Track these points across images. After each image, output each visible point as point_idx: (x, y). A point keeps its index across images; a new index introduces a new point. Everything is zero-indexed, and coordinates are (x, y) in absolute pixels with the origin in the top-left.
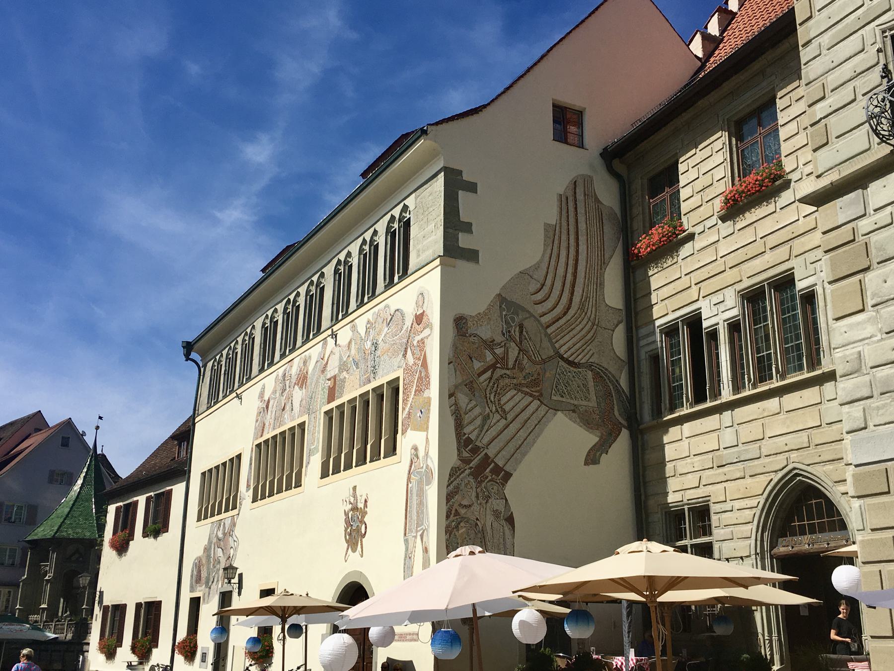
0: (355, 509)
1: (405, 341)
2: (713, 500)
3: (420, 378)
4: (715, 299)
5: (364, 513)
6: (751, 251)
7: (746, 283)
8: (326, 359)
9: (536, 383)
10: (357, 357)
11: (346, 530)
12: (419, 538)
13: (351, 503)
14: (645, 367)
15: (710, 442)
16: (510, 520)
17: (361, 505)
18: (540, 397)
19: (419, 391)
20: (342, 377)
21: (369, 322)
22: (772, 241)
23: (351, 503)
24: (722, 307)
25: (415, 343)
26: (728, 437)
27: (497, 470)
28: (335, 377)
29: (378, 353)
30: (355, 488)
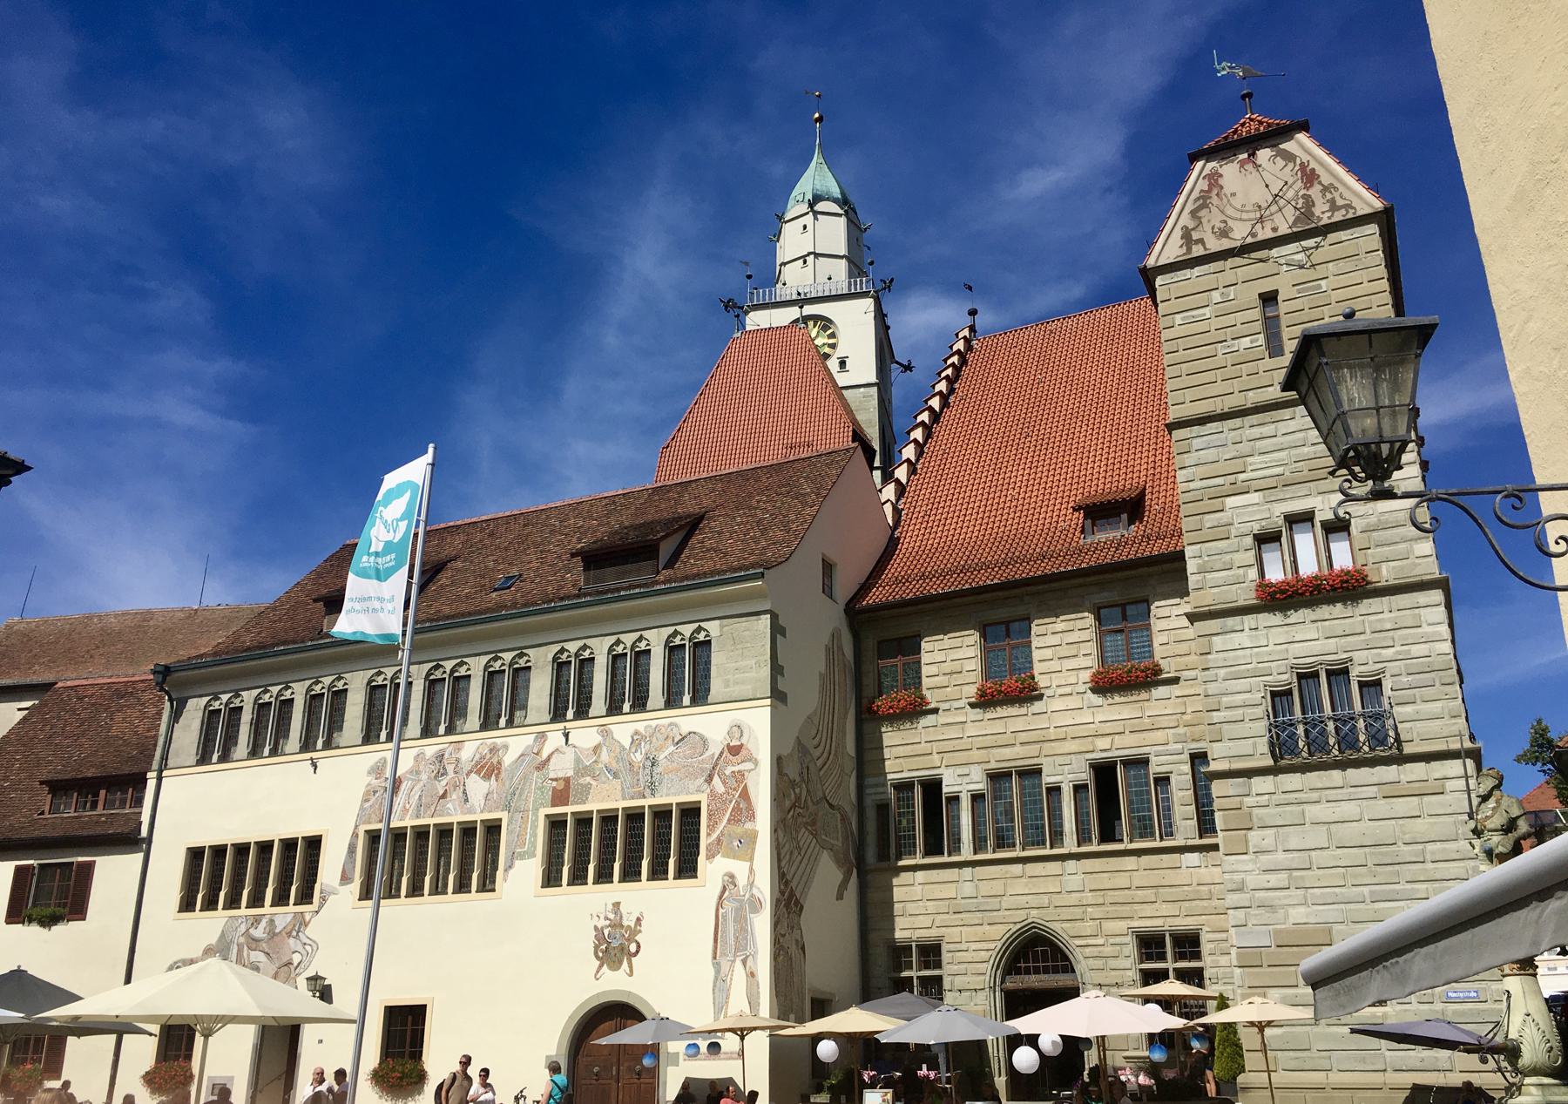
0: (617, 925)
1: (710, 766)
2: (946, 939)
3: (736, 809)
4: (960, 771)
5: (634, 931)
6: (1001, 740)
7: (993, 765)
8: (545, 755)
9: (814, 823)
10: (614, 766)
11: (596, 948)
12: (738, 964)
13: (606, 918)
14: (871, 814)
15: (949, 891)
16: (803, 949)
17: (629, 921)
18: (815, 836)
19: (735, 819)
20: (581, 781)
21: (636, 733)
22: (1023, 737)
23: (606, 918)
24: (967, 779)
25: (728, 772)
26: (968, 889)
27: (797, 902)
28: (567, 780)
29: (657, 770)
30: (617, 905)
